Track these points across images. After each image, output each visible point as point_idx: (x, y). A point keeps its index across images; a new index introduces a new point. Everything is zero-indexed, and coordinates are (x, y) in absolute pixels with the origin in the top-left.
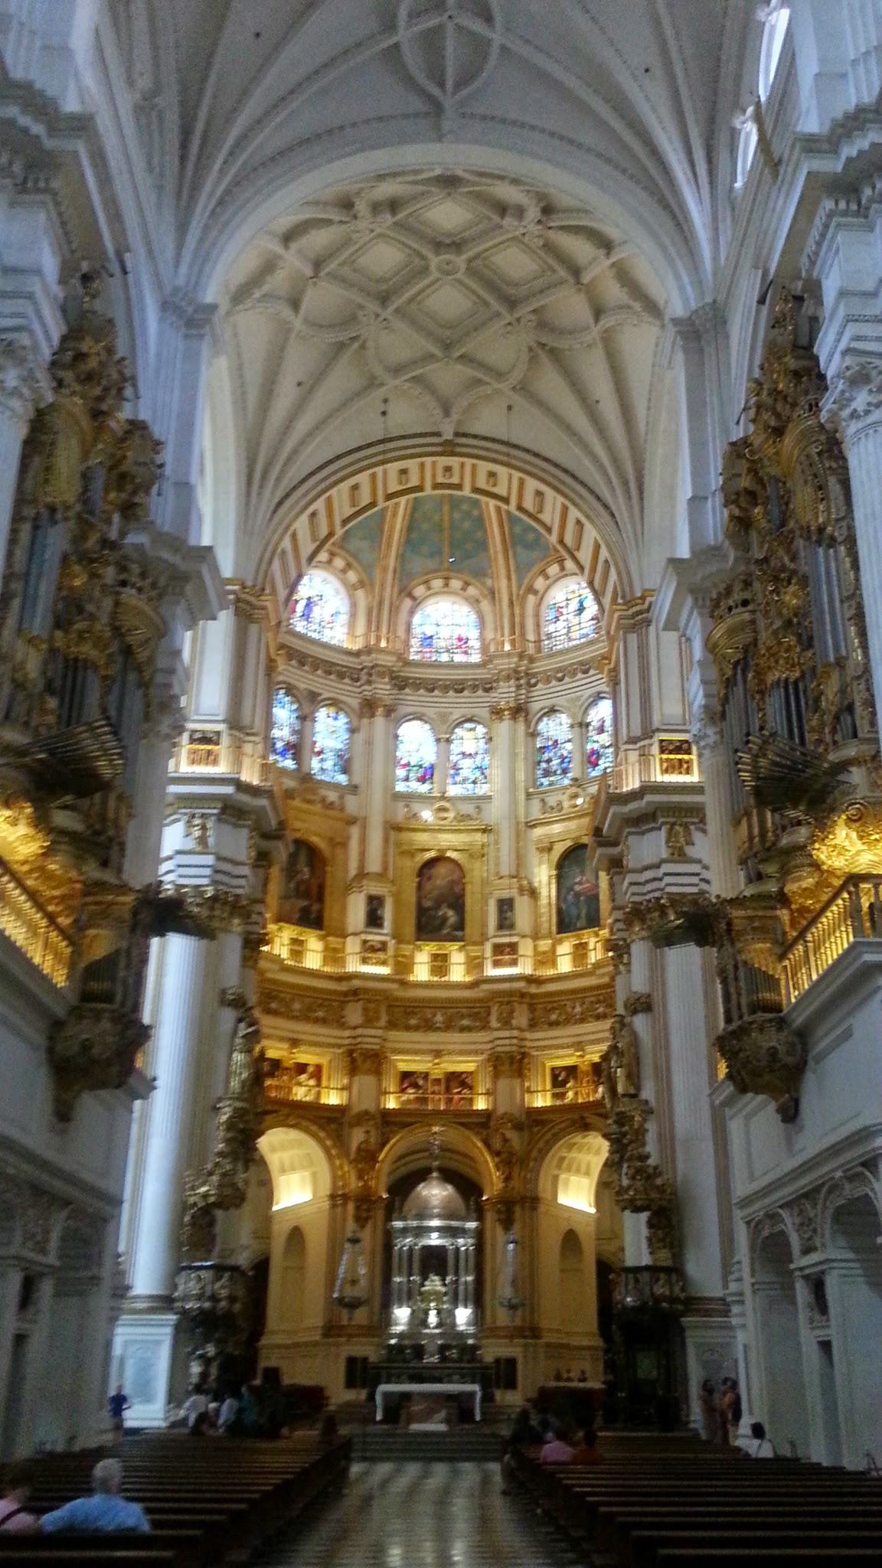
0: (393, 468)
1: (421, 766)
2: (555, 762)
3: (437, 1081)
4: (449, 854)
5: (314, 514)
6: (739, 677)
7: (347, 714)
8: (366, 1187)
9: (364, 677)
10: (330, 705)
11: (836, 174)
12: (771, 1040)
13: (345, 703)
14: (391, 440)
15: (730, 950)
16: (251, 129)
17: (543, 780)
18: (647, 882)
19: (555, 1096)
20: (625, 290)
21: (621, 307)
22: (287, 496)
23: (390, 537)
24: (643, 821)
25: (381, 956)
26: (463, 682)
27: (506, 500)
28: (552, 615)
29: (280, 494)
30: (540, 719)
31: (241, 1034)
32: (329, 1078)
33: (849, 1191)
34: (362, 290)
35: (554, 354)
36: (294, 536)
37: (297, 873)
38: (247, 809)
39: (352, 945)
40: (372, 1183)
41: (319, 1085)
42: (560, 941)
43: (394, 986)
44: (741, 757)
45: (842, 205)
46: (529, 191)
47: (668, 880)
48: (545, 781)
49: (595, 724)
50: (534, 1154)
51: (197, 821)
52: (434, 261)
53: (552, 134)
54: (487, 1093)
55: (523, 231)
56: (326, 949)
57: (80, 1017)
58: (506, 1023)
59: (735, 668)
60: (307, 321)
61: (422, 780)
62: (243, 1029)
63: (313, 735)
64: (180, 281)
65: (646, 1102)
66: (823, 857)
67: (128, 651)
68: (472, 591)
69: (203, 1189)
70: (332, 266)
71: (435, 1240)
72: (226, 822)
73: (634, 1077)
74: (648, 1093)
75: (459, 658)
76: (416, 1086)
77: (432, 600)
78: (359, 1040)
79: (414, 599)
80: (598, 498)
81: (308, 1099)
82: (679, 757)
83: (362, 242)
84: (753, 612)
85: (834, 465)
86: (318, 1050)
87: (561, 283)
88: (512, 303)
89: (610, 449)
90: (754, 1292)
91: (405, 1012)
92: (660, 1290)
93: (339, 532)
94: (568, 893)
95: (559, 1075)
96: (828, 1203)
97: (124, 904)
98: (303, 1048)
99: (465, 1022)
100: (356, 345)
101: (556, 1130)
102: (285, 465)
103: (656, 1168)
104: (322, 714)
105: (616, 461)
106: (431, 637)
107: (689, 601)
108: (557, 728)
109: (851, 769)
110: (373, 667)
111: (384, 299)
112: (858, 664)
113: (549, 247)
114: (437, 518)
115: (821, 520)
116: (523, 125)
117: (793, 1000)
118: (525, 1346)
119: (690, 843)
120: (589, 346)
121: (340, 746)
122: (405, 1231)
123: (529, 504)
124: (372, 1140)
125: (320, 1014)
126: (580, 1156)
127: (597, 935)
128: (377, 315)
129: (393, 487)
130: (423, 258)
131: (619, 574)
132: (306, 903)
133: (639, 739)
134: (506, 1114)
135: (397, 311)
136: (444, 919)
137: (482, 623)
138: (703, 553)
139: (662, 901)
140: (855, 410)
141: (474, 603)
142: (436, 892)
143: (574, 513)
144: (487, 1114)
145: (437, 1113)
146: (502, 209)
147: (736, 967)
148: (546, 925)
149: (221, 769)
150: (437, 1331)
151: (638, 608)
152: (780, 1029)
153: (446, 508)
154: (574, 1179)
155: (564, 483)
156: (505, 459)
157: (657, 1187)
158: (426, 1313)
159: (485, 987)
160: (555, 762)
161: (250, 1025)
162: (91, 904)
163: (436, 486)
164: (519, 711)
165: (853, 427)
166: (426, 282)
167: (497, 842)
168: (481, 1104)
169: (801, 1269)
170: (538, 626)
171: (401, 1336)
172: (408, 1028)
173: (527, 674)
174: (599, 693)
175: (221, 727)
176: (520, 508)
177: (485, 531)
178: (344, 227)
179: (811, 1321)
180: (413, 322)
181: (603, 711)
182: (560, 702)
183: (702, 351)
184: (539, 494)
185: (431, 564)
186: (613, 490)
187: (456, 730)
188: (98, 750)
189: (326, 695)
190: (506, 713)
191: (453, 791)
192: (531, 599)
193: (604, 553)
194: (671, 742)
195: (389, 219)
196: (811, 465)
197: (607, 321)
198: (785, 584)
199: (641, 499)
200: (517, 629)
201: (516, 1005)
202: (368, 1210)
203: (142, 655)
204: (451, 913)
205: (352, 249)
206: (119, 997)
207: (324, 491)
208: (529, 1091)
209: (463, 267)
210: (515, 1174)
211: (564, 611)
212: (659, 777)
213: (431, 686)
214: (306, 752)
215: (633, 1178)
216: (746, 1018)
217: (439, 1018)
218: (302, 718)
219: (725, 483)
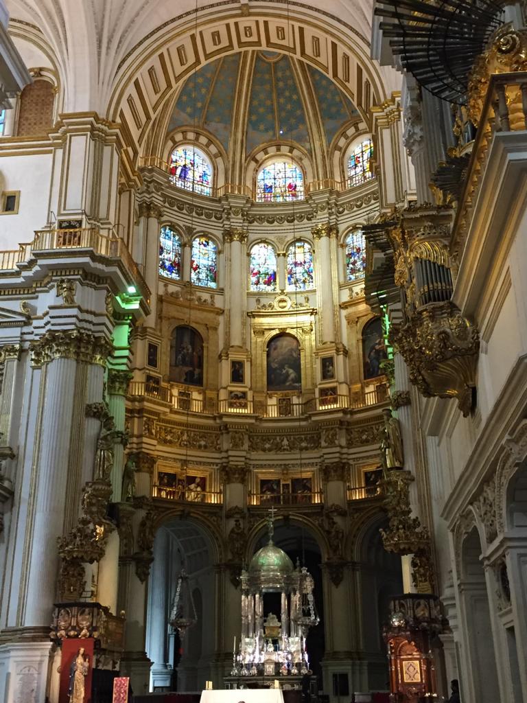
1: (267, 274)
7: (214, 241)
9: (225, 216)
10: (202, 236)
13: (211, 234)
14: (203, 8)
17: (351, 276)
19: (368, 491)
23: (237, 120)
25: (242, 401)
26: (293, 214)
27: (293, 50)
28: (353, 164)
30: (347, 235)
36: (137, 84)
37: (184, 348)
48: (353, 277)
54: (321, 492)
56: (205, 398)
58: (331, 443)
61: (268, 283)
63: (192, 257)
65: (409, 472)
68: (296, 152)
72: (88, 285)
74: (410, 466)
75: (289, 199)
76: (272, 490)
77: (270, 162)
78: (231, 459)
79: (257, 161)
91: (262, 438)
94: (371, 351)
95: (371, 477)
98: (190, 466)
103: (415, 520)
104: (196, 243)
106: (271, 187)
114: (268, 103)
121: (210, 263)
125: (203, 443)
132: (191, 369)
134: (333, 505)
136: (288, 375)
137: (304, 174)
141: (298, 161)
142: (280, 358)
144: (321, 506)
148: (357, 374)
153: (274, 95)
164: (331, 230)
169: (488, 558)
170: (343, 171)
172: (264, 450)
173: (336, 205)
177: (303, 109)
187: (291, 248)
189: (199, 229)
190: (323, 232)
192: (337, 154)
200: (329, 175)
204: (291, 371)
208: (350, 489)
211: (361, 159)
217: (285, 442)
218: (183, 245)
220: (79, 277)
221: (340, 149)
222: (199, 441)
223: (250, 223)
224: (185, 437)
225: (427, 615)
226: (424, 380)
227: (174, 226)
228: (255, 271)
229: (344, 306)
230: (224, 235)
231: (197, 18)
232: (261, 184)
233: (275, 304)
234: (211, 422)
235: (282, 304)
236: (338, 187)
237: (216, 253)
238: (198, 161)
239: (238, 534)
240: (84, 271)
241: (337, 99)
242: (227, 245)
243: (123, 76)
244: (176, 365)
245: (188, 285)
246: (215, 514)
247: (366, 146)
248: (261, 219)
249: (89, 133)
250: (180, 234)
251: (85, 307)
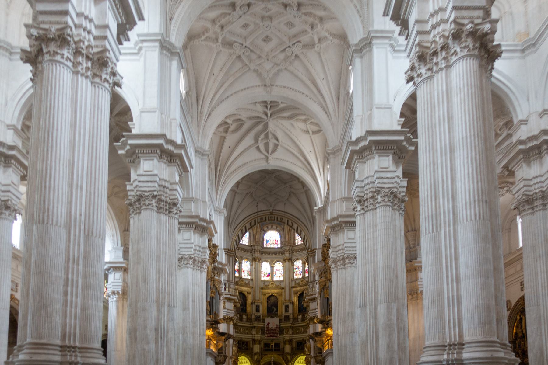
22: (236, 227)
26: (277, 252)
61: (268, 276)
68: (278, 228)
75: (276, 246)
80: (305, 225)
137: (281, 237)
141: (279, 232)
143: (299, 228)
167: (285, 292)
176: (288, 224)
186: (308, 224)
191: (275, 279)
193: (306, 238)
213: (269, 253)
245: (240, 278)
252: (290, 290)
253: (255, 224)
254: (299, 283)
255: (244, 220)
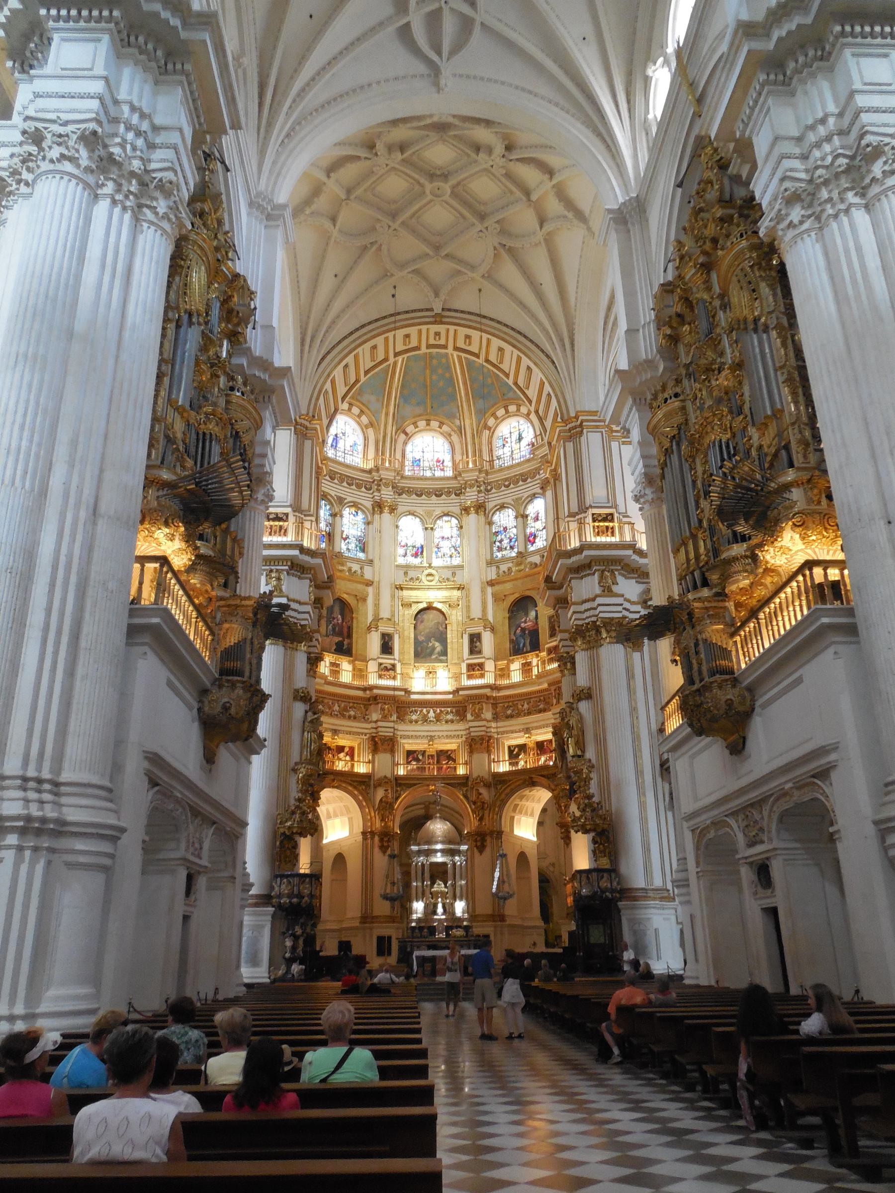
0: (400, 333)
1: (414, 547)
2: (506, 542)
3: (432, 756)
4: (435, 605)
5: (346, 366)
6: (674, 447)
7: (363, 512)
8: (386, 826)
11: (769, 51)
12: (731, 694)
13: (361, 504)
14: (399, 314)
15: (691, 632)
16: (308, 84)
18: (586, 610)
19: (510, 764)
20: (562, 204)
21: (559, 217)
22: (329, 353)
23: (390, 393)
24: (581, 570)
26: (441, 489)
28: (501, 443)
29: (323, 352)
31: (309, 719)
32: (359, 756)
33: (798, 797)
34: (379, 209)
35: (511, 251)
36: (333, 382)
37: (334, 618)
38: (307, 566)
39: (372, 667)
40: (391, 824)
41: (352, 759)
42: (513, 661)
43: (403, 693)
44: (714, 480)
45: (772, 77)
46: (496, 133)
47: (600, 609)
48: (499, 555)
49: (532, 515)
50: (498, 803)
51: (273, 575)
52: (428, 187)
53: (517, 87)
54: (466, 763)
55: (491, 163)
56: (354, 669)
57: (220, 687)
58: (478, 716)
59: (671, 442)
60: (340, 231)
61: (416, 555)
62: (310, 717)
64: (262, 187)
66: (768, 557)
67: (236, 436)
69: (289, 824)
70: (359, 192)
71: (439, 858)
72: (293, 575)
73: (581, 745)
74: (590, 754)
75: (438, 474)
76: (418, 760)
78: (380, 729)
79: (406, 434)
80: (543, 351)
81: (346, 769)
82: (606, 524)
83: (380, 173)
84: (683, 401)
85: (764, 275)
86: (351, 737)
87: (517, 202)
88: (482, 217)
89: (550, 317)
90: (698, 878)
92: (604, 884)
93: (363, 379)
96: (775, 809)
97: (247, 606)
98: (340, 735)
99: (449, 717)
100: (374, 248)
101: (512, 786)
102: (327, 331)
104: (346, 512)
105: (554, 325)
106: (419, 460)
107: (630, 401)
108: (506, 519)
109: (793, 490)
110: (381, 480)
111: (394, 216)
112: (790, 414)
113: (508, 176)
115: (756, 314)
116: (496, 81)
117: (743, 666)
118: (495, 927)
119: (615, 583)
120: (536, 245)
121: (359, 534)
122: (419, 853)
123: (493, 358)
124: (390, 795)
125: (352, 713)
126: (528, 804)
127: (537, 656)
128: (389, 227)
129: (400, 347)
130: (422, 185)
131: (558, 402)
132: (341, 639)
133: (577, 514)
135: (403, 223)
136: (434, 649)
138: (638, 366)
139: (598, 623)
140: (791, 222)
143: (525, 362)
144: (466, 778)
145: (433, 779)
146: (477, 149)
147: (696, 645)
149: (289, 538)
150: (444, 917)
151: (573, 424)
152: (734, 686)
154: (523, 818)
155: (519, 341)
156: (478, 326)
157: (600, 816)
158: (435, 906)
159: (461, 693)
160: (506, 542)
161: (315, 713)
162: (223, 606)
163: (429, 346)
164: (480, 507)
165: (791, 233)
166: (424, 202)
167: (467, 596)
168: (461, 771)
169: (746, 858)
171: (419, 920)
174: (534, 494)
175: (288, 510)
178: (368, 162)
179: (756, 893)
180: (414, 232)
181: (538, 506)
182: (509, 500)
183: (629, 231)
184: (501, 349)
185: (418, 410)
187: (438, 522)
188: (232, 482)
189: (349, 499)
191: (436, 562)
192: (486, 433)
193: (547, 388)
194: (600, 515)
195: (399, 156)
196: (746, 276)
197: (548, 227)
198: (716, 372)
199: (573, 350)
200: (478, 452)
201: (484, 705)
202: (389, 841)
203: (246, 439)
204: (437, 644)
205: (374, 178)
206: (247, 674)
207: (354, 349)
209: (449, 191)
210: (486, 815)
211: (509, 440)
212: (591, 537)
214: (337, 538)
215: (584, 810)
216: (707, 679)
218: (334, 515)
219: (656, 316)
220: (287, 568)
221: (489, 429)
222: (348, 711)
223: (399, 495)
224: (336, 708)
225: (609, 885)
226: (701, 727)
227: (325, 496)
228: (403, 544)
229: (491, 583)
230: (373, 508)
231: (395, 322)
232: (409, 456)
233: (424, 578)
234: (360, 693)
235: (430, 578)
236: (486, 466)
237: (365, 523)
238: (349, 430)
239: (387, 803)
240: (292, 563)
241: (489, 381)
242: (377, 516)
243: (323, 372)
244: (327, 636)
246: (363, 783)
247: (515, 427)
248: (409, 491)
249: (293, 428)
250: (331, 503)
251: (291, 596)
252: (483, 591)
253: (386, 359)
254: (509, 569)
255: (351, 333)
